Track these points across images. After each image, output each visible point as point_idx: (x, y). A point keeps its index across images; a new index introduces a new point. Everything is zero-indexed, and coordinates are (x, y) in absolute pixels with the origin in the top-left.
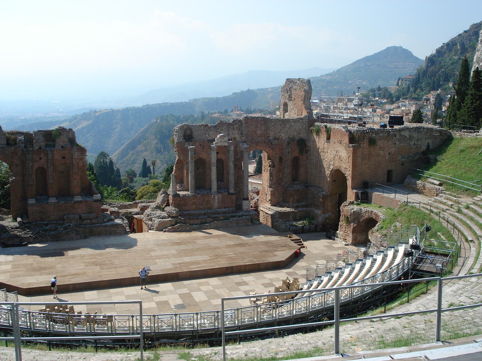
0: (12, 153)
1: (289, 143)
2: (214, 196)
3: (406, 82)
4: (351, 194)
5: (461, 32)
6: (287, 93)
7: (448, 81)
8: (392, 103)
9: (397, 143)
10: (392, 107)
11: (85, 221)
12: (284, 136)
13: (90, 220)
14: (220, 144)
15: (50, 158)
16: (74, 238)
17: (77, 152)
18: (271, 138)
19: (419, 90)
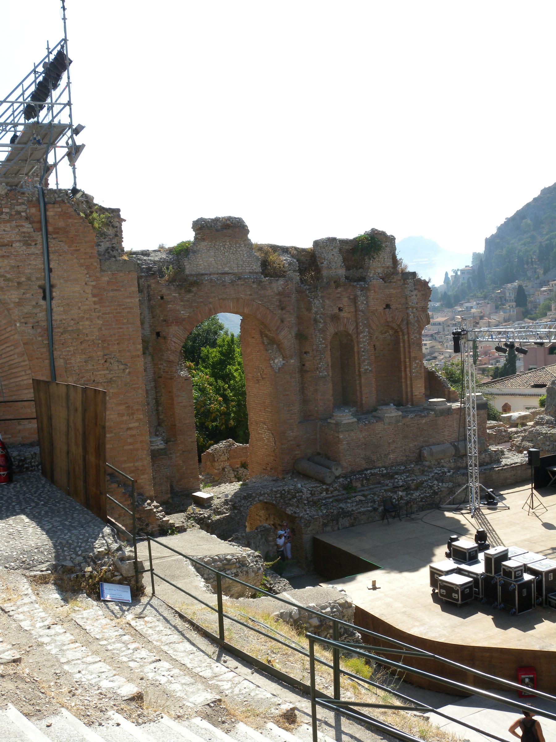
0: (279, 294)
15: (362, 307)
17: (415, 293)
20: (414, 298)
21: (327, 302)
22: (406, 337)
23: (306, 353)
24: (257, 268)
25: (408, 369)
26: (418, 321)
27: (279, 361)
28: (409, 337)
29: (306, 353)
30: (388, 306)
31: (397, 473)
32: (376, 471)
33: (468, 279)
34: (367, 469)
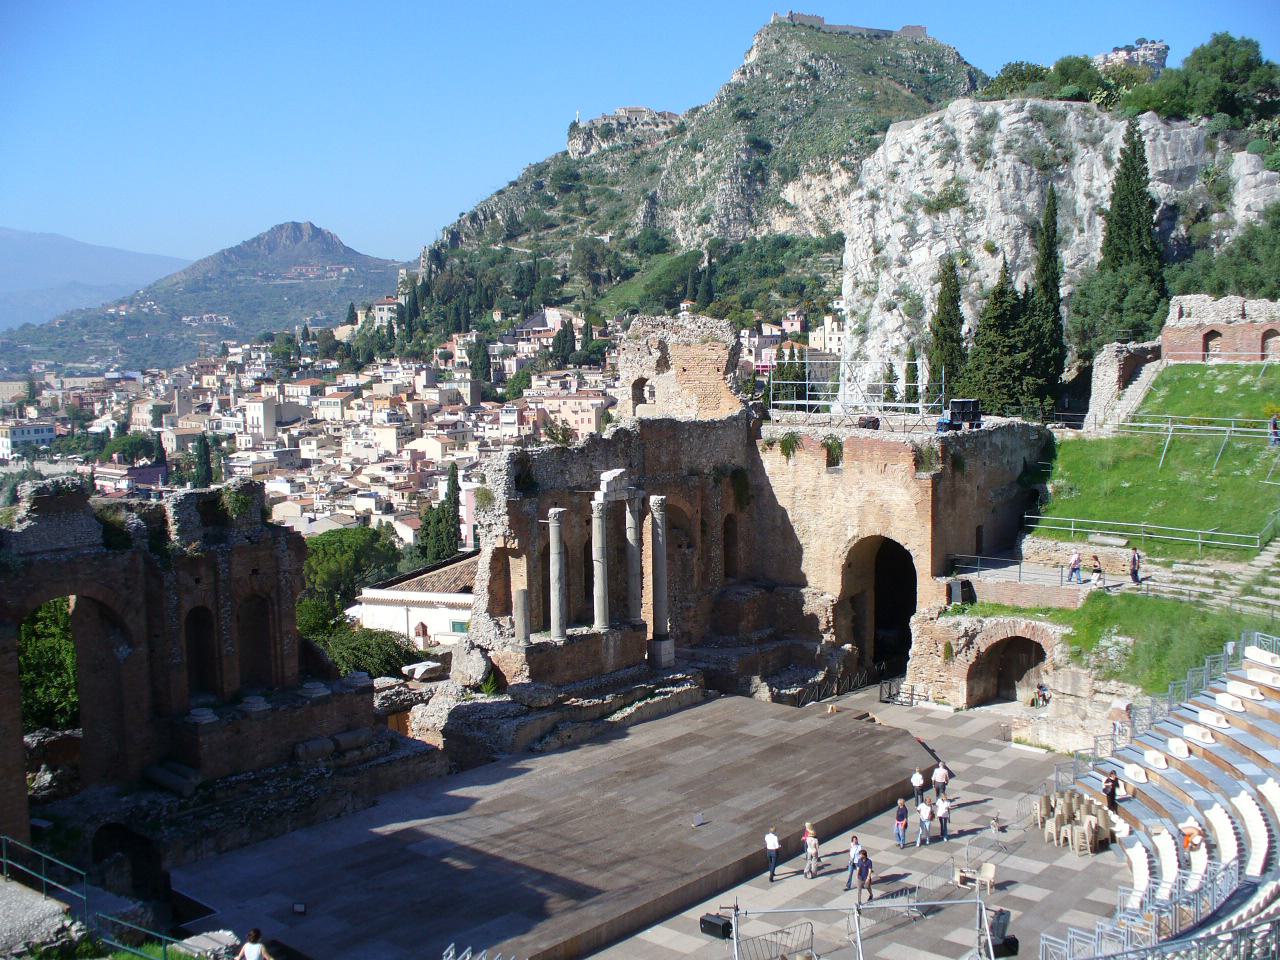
1: (716, 481)
2: (607, 639)
3: (381, 314)
4: (930, 591)
5: (503, 184)
6: (650, 354)
7: (490, 307)
8: (358, 369)
9: (988, 462)
10: (363, 379)
11: (348, 756)
12: (706, 465)
13: (359, 748)
14: (612, 498)
15: (222, 576)
16: (349, 808)
17: (288, 552)
18: (685, 473)
19: (419, 333)
20: (287, 560)
21: (181, 573)
22: (276, 607)
23: (156, 636)
24: (97, 537)
25: (278, 647)
26: (291, 587)
27: (123, 651)
28: (280, 606)
29: (156, 636)
30: (255, 572)
31: (266, 778)
32: (242, 777)
33: (390, 322)
34: (232, 776)
